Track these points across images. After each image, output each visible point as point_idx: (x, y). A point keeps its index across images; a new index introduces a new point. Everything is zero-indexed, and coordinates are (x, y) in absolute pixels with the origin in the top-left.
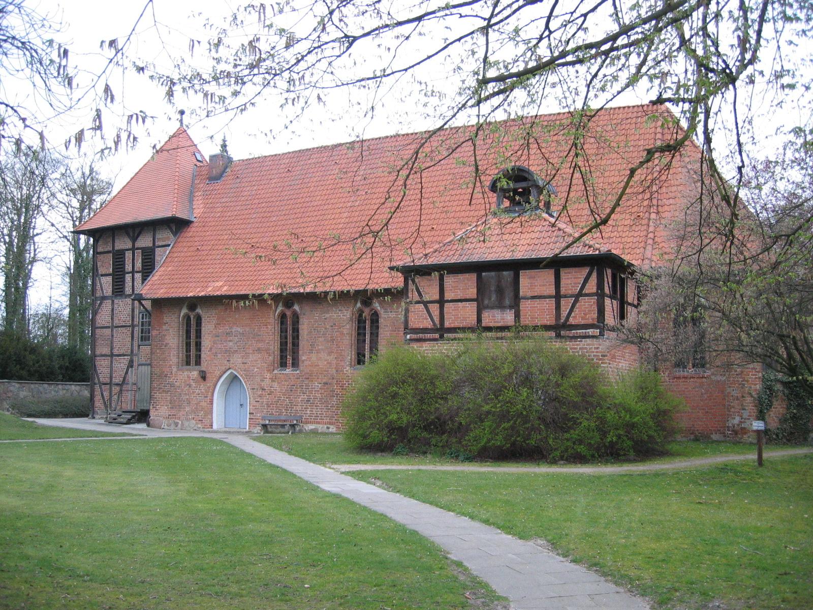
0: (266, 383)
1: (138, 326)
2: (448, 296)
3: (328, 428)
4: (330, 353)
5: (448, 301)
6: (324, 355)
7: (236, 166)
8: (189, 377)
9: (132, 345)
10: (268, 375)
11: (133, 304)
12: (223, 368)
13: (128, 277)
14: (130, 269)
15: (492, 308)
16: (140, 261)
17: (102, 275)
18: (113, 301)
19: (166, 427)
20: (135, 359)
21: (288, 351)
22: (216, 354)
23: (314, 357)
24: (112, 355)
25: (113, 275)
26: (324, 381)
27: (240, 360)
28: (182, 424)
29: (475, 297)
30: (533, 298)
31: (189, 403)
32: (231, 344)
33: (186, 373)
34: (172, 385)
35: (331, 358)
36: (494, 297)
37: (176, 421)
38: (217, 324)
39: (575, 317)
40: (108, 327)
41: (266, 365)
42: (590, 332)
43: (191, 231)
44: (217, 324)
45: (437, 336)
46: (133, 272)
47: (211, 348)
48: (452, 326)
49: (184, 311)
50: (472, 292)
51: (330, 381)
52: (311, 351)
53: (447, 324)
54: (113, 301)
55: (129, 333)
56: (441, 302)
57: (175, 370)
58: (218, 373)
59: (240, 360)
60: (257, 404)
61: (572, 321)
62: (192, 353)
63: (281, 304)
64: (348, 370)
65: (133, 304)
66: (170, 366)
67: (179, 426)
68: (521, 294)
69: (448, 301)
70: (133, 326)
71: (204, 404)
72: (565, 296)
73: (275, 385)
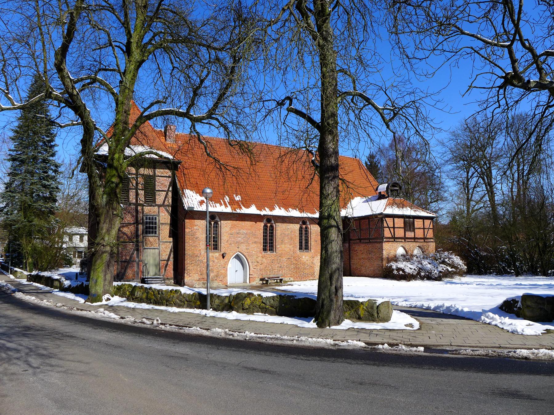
0: (259, 259)
4: (291, 244)
6: (288, 246)
21: (269, 243)
22: (231, 244)
23: (283, 246)
32: (240, 239)
52: (282, 243)
61: (428, 237)
64: (298, 251)
66: (200, 250)
71: (223, 271)
73: (264, 260)
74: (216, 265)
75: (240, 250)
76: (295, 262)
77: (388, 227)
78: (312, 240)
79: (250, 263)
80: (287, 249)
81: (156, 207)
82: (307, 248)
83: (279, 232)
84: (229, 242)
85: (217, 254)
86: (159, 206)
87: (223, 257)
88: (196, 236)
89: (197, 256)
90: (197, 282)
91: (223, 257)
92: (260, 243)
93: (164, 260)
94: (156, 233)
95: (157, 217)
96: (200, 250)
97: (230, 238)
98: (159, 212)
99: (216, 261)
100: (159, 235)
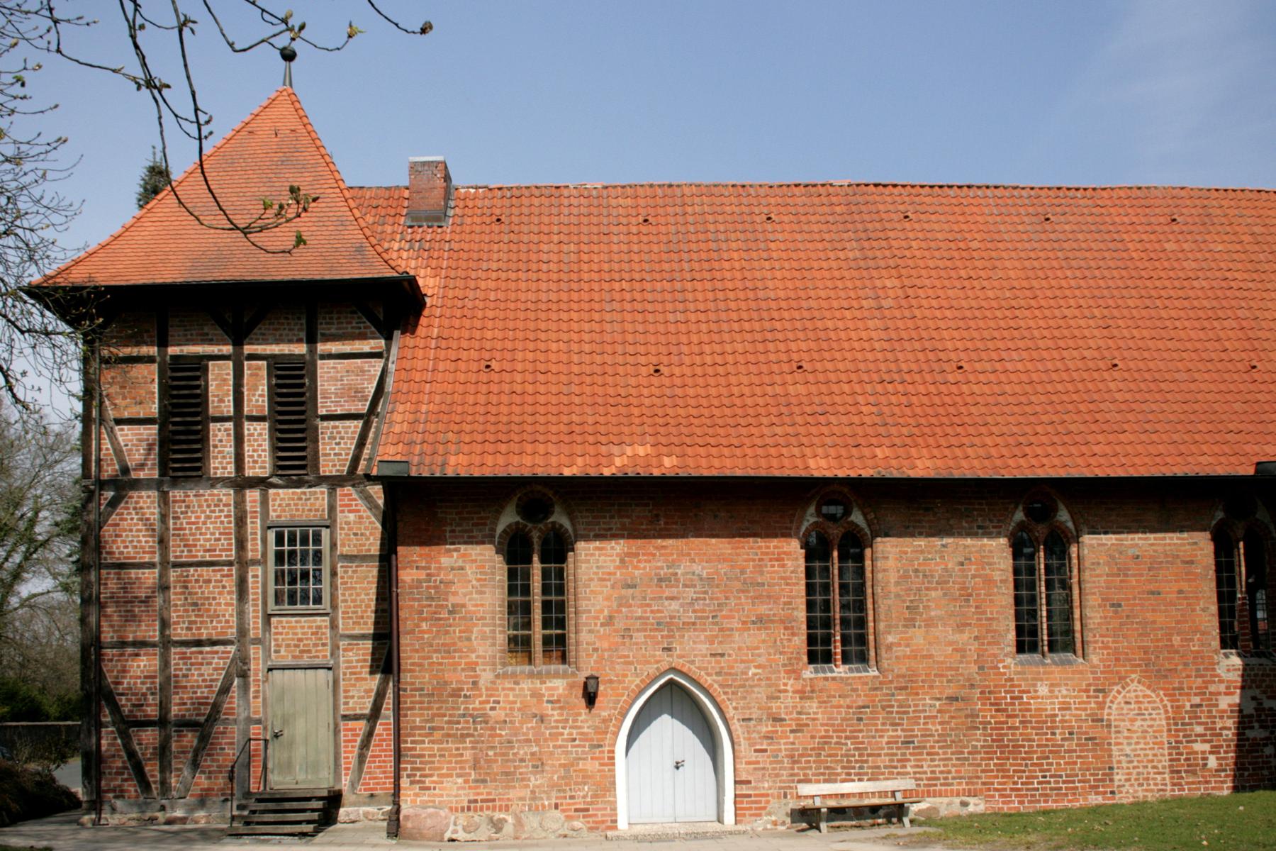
0: (786, 704)
1: (263, 562)
4: (961, 627)
6: (945, 633)
8: (536, 694)
9: (241, 614)
10: (791, 684)
11: (240, 503)
12: (652, 669)
13: (220, 435)
14: (228, 408)
16: (263, 388)
17: (119, 422)
18: (164, 497)
19: (461, 835)
20: (254, 652)
22: (627, 633)
23: (918, 636)
24: (166, 643)
25: (163, 420)
27: (704, 648)
28: (519, 823)
31: (539, 766)
32: (675, 605)
33: (526, 685)
35: (964, 637)
37: (498, 815)
38: (629, 555)
40: (151, 565)
41: (782, 659)
43: (430, 324)
44: (629, 555)
46: (238, 418)
47: (611, 618)
49: (508, 518)
51: (963, 692)
52: (910, 623)
55: (231, 584)
57: (486, 677)
59: (704, 648)
62: (540, 625)
64: (1011, 663)
65: (240, 503)
66: (472, 667)
67: (508, 829)
70: (242, 563)
71: (591, 766)
73: (813, 706)
74: (554, 736)
75: (678, 662)
76: (989, 716)
78: (1092, 601)
79: (737, 726)
80: (941, 653)
81: (322, 491)
82: (1064, 640)
83: (891, 563)
84: (620, 624)
85: (559, 685)
86: (334, 482)
87: (590, 698)
89: (456, 693)
90: (462, 819)
91: (590, 698)
92: (787, 624)
93: (357, 718)
94: (318, 600)
95: (325, 534)
96: (472, 667)
97: (623, 602)
98: (332, 508)
99: (556, 715)
100: (334, 606)
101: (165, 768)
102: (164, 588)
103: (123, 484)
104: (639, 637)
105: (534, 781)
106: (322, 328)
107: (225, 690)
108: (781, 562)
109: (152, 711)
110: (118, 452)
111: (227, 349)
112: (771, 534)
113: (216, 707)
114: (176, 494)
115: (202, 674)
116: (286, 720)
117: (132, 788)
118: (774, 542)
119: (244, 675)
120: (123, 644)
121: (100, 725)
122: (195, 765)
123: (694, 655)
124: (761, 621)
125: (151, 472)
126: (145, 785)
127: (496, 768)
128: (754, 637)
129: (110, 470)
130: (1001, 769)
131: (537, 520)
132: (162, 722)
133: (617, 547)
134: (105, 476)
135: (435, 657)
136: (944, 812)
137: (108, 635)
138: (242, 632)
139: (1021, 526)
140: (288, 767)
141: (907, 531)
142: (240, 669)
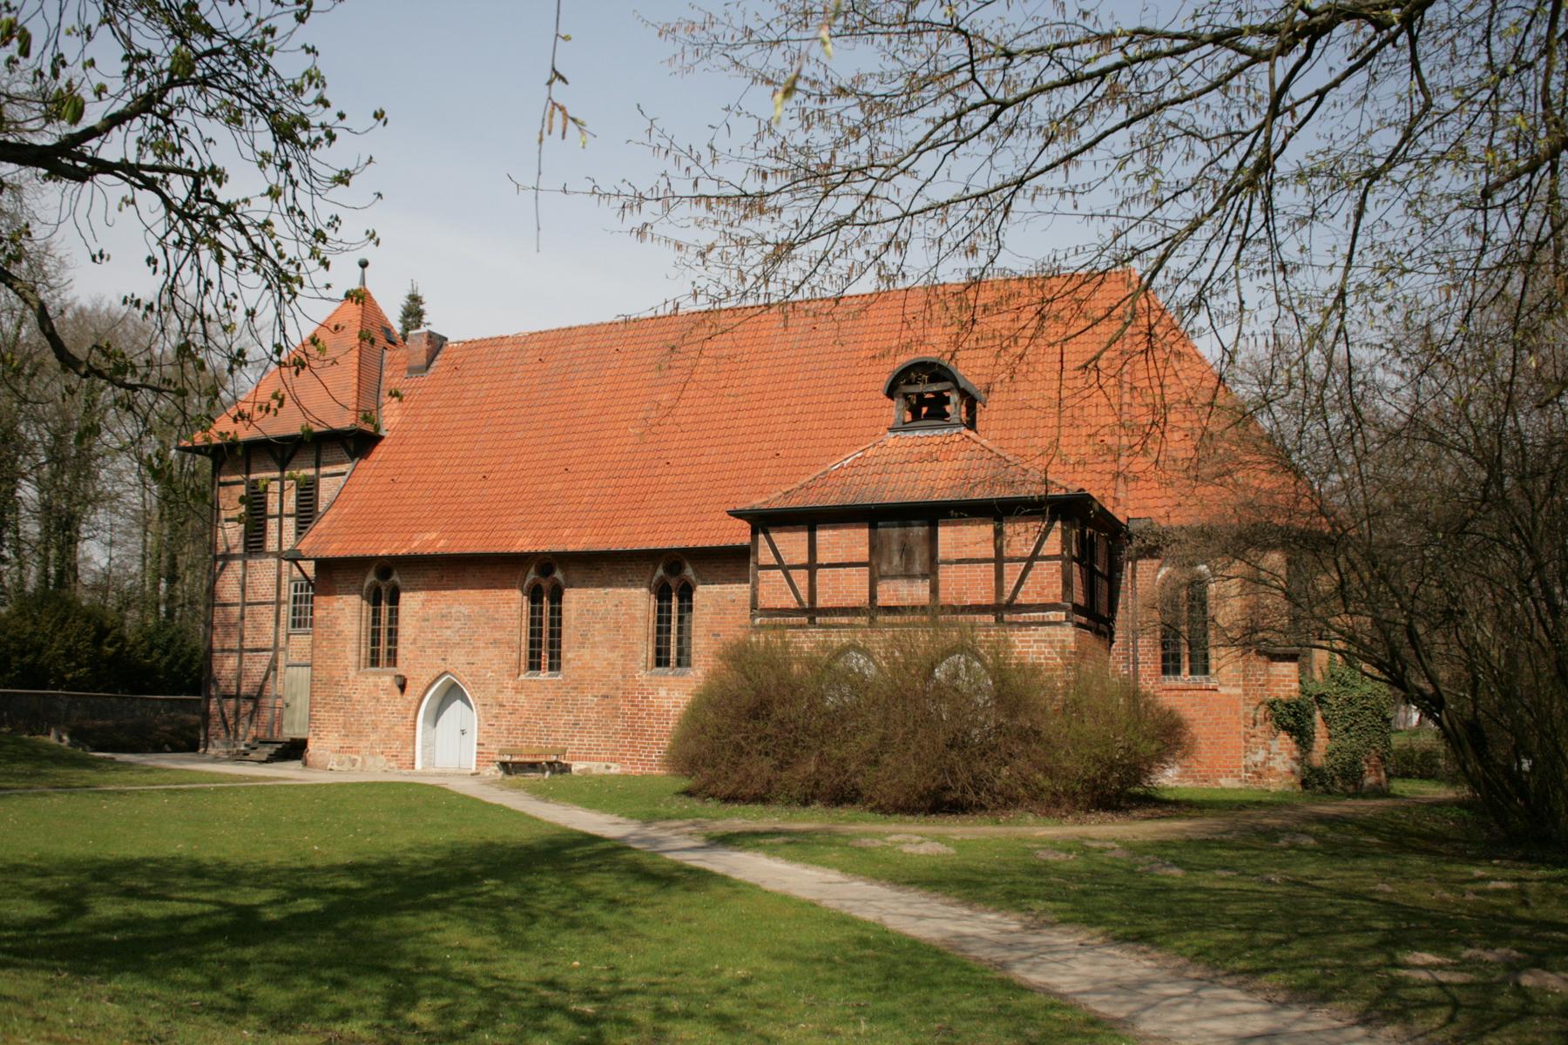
2: (822, 558)
3: (608, 767)
4: (613, 648)
5: (822, 566)
6: (603, 652)
7: (453, 350)
8: (376, 685)
9: (276, 633)
10: (511, 683)
11: (280, 566)
12: (436, 672)
13: (272, 525)
14: (276, 511)
15: (894, 577)
18: (245, 563)
19: (335, 767)
20: (281, 656)
21: (544, 647)
23: (586, 654)
24: (242, 650)
26: (603, 692)
27: (463, 659)
29: (866, 559)
30: (959, 561)
31: (375, 729)
32: (449, 632)
33: (371, 679)
34: (348, 699)
35: (613, 656)
36: (896, 560)
39: (1026, 593)
42: (1051, 615)
43: (379, 452)
45: (805, 620)
48: (830, 604)
49: (371, 578)
50: (862, 552)
51: (612, 693)
52: (582, 645)
53: (820, 603)
54: (245, 563)
55: (272, 616)
56: (812, 566)
58: (426, 680)
59: (463, 659)
60: (491, 729)
61: (1021, 599)
63: (532, 570)
64: (642, 675)
65: (280, 566)
67: (358, 765)
68: (941, 555)
69: (822, 566)
70: (279, 603)
71: (401, 729)
72: (1011, 560)
73: (522, 698)
76: (627, 709)
77: (780, 565)
84: (420, 644)
87: (402, 687)
88: (339, 628)
89: (337, 684)
90: (336, 757)
91: (402, 687)
92: (509, 644)
97: (422, 630)
99: (384, 698)
101: (236, 723)
102: (242, 618)
103: (227, 557)
104: (429, 652)
105: (373, 737)
106: (324, 458)
107: (266, 678)
108: (511, 605)
109: (233, 689)
110: (226, 539)
111: (277, 474)
112: (504, 586)
113: (262, 688)
114: (250, 562)
115: (257, 667)
116: (294, 697)
117: (223, 734)
118: (506, 592)
119: (275, 669)
120: (223, 650)
121: (211, 697)
122: (251, 720)
123: (458, 664)
124: (495, 642)
125: (239, 550)
126: (228, 732)
127: (354, 728)
128: (492, 652)
129: (221, 549)
130: (632, 745)
131: (382, 579)
132: (237, 696)
133: (421, 596)
134: (219, 553)
135: (329, 662)
136: (594, 772)
137: (217, 645)
138: (276, 644)
139: (661, 579)
140: (292, 724)
141: (584, 584)
142: (273, 666)
